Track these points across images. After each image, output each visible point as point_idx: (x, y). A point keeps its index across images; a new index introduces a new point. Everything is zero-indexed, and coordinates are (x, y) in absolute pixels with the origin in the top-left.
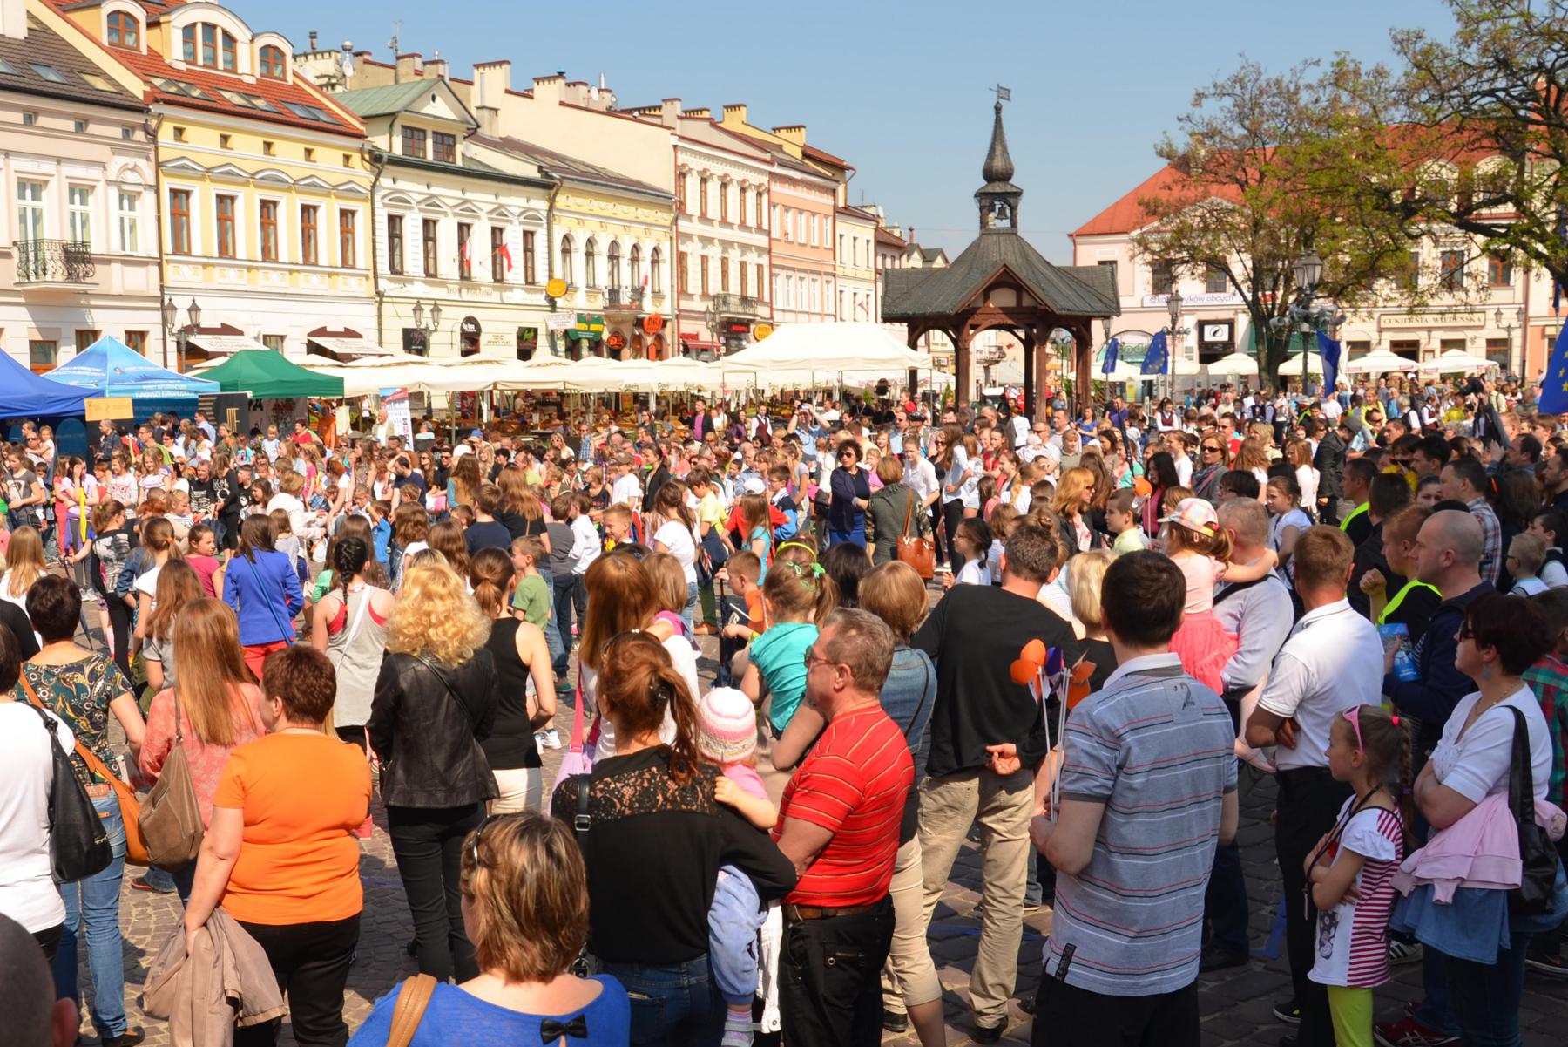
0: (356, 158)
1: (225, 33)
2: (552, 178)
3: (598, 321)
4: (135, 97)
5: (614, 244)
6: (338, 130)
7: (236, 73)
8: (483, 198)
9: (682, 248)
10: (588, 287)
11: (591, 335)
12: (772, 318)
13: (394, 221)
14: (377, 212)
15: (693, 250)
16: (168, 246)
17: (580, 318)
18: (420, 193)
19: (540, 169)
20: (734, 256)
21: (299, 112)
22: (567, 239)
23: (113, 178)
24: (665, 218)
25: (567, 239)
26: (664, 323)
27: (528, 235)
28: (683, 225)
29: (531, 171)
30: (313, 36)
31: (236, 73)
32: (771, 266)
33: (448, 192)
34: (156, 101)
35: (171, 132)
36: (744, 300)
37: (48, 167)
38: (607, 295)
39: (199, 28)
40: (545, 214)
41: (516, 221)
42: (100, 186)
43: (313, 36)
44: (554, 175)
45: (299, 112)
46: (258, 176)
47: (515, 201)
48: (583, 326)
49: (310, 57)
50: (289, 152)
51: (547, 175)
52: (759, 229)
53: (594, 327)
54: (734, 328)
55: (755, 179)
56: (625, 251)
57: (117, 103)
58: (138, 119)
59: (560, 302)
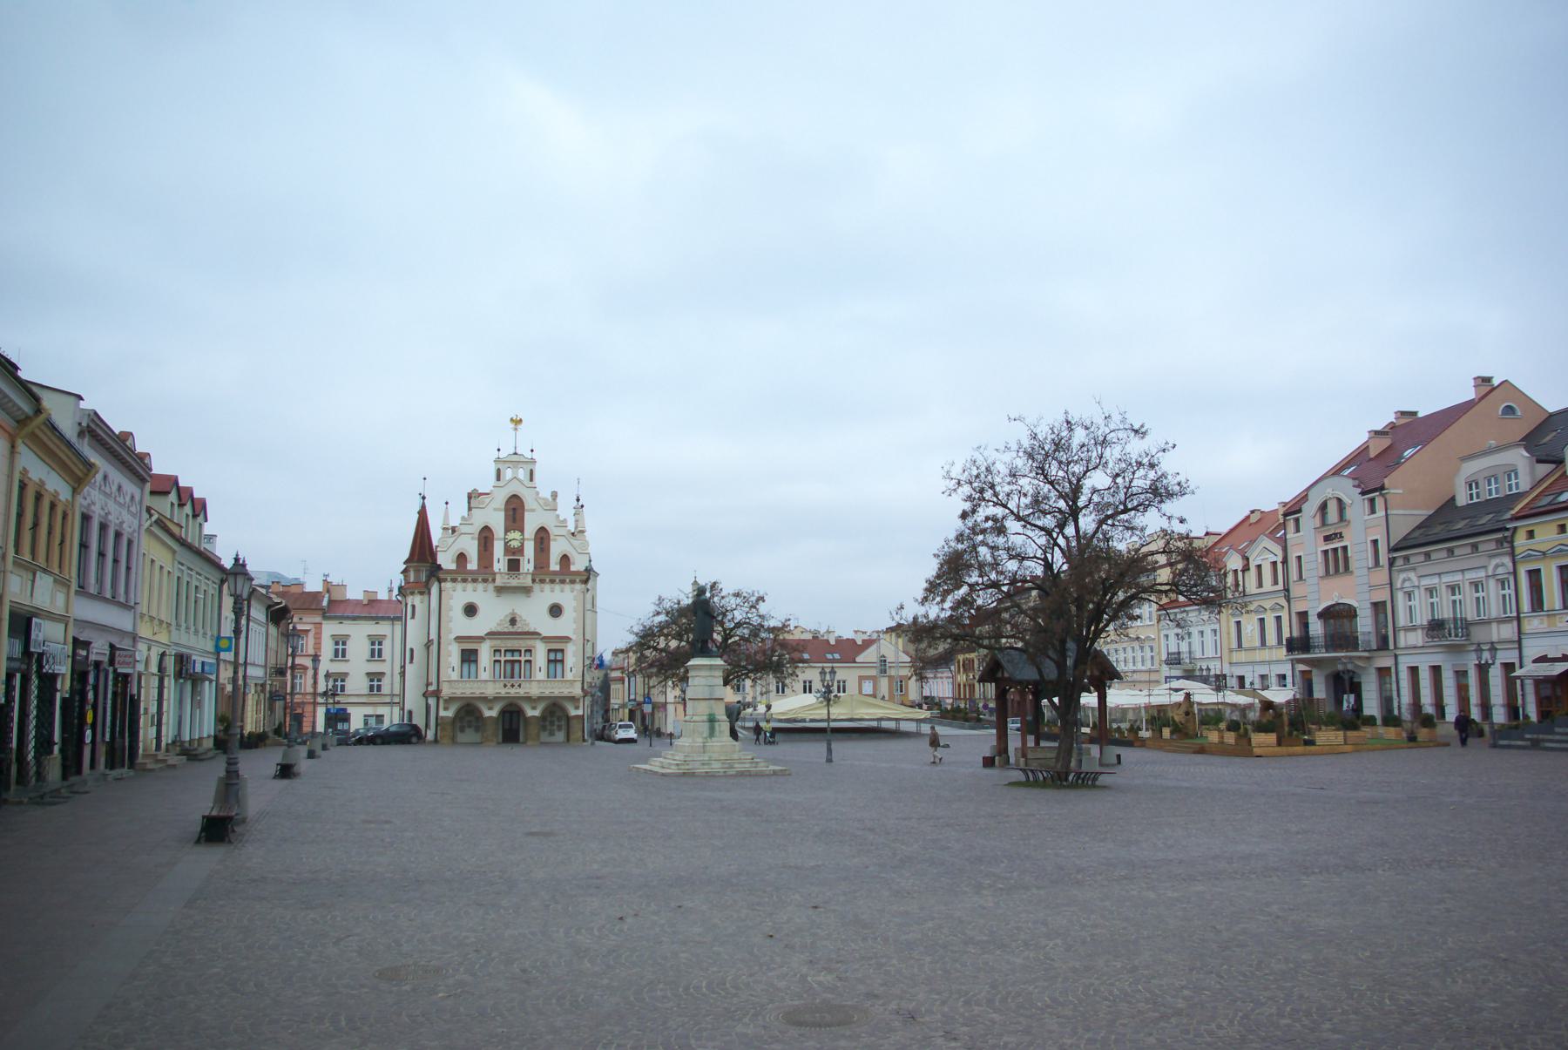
23: (1490, 574)
37: (1435, 580)
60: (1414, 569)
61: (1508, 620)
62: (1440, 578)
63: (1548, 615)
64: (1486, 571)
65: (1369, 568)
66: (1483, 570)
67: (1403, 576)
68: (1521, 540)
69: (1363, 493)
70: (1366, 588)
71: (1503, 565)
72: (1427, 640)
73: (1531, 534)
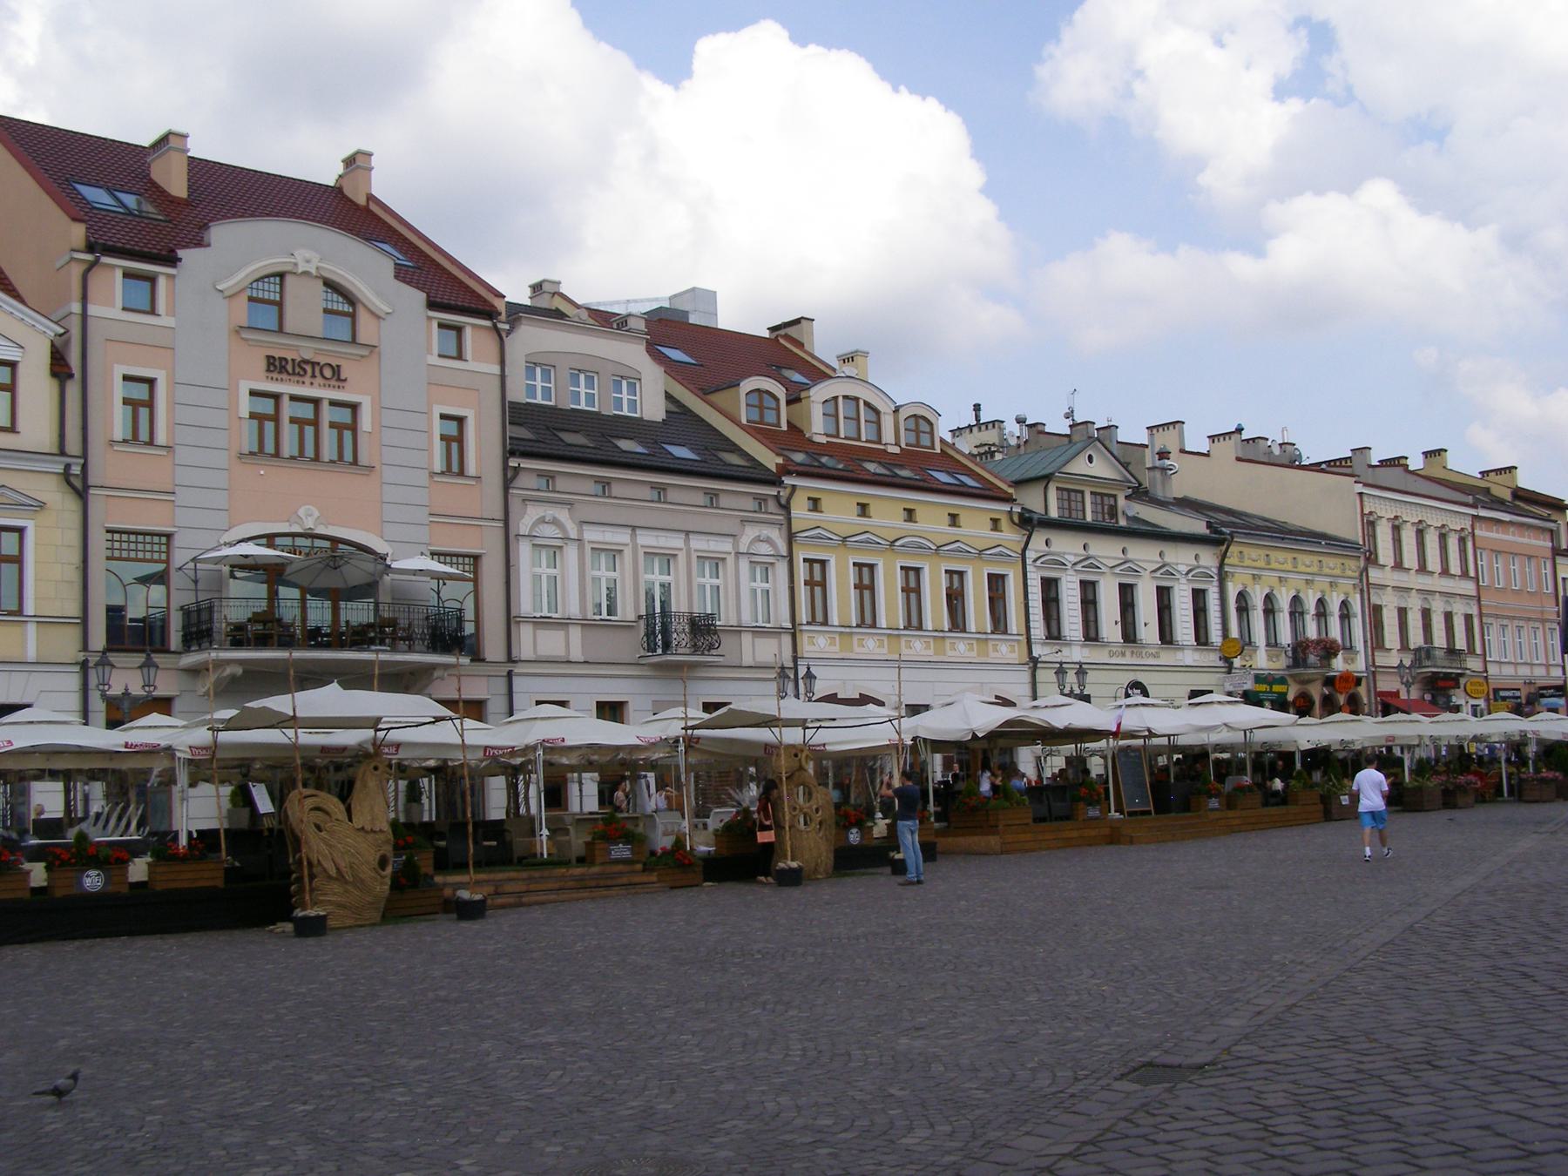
0: (1004, 523)
1: (867, 404)
2: (1222, 533)
3: (1282, 681)
4: (769, 470)
5: (1296, 600)
6: (988, 493)
7: (879, 442)
8: (1145, 554)
9: (1375, 600)
10: (1268, 645)
11: (1274, 697)
12: (1486, 671)
13: (1050, 586)
14: (1029, 575)
15: (1389, 604)
16: (803, 615)
17: (1258, 679)
18: (1076, 555)
19: (1209, 525)
20: (1438, 607)
21: (944, 478)
22: (1242, 596)
23: (743, 549)
24: (1353, 566)
25: (1242, 596)
26: (1358, 681)
27: (1199, 596)
28: (1375, 575)
29: (1198, 526)
30: (977, 408)
31: (879, 442)
32: (1481, 615)
33: (1106, 550)
34: (789, 473)
35: (806, 504)
36: (1451, 651)
38: (1290, 654)
39: (840, 399)
40: (1215, 570)
41: (1183, 580)
42: (730, 560)
43: (977, 408)
44: (1224, 529)
45: (944, 478)
46: (897, 544)
47: (1182, 557)
48: (1263, 687)
49: (975, 429)
50: (932, 515)
51: (1216, 531)
52: (1465, 574)
53: (1276, 688)
54: (1441, 684)
55: (1456, 524)
57: (754, 475)
58: (773, 491)
59: (1237, 662)
60: (570, 504)
61: (776, 632)
62: (633, 536)
63: (978, 639)
64: (735, 545)
65: (433, 474)
66: (730, 540)
67: (533, 513)
68: (800, 510)
69: (432, 305)
70: (183, 496)
71: (768, 541)
72: (643, 653)
73: (815, 504)
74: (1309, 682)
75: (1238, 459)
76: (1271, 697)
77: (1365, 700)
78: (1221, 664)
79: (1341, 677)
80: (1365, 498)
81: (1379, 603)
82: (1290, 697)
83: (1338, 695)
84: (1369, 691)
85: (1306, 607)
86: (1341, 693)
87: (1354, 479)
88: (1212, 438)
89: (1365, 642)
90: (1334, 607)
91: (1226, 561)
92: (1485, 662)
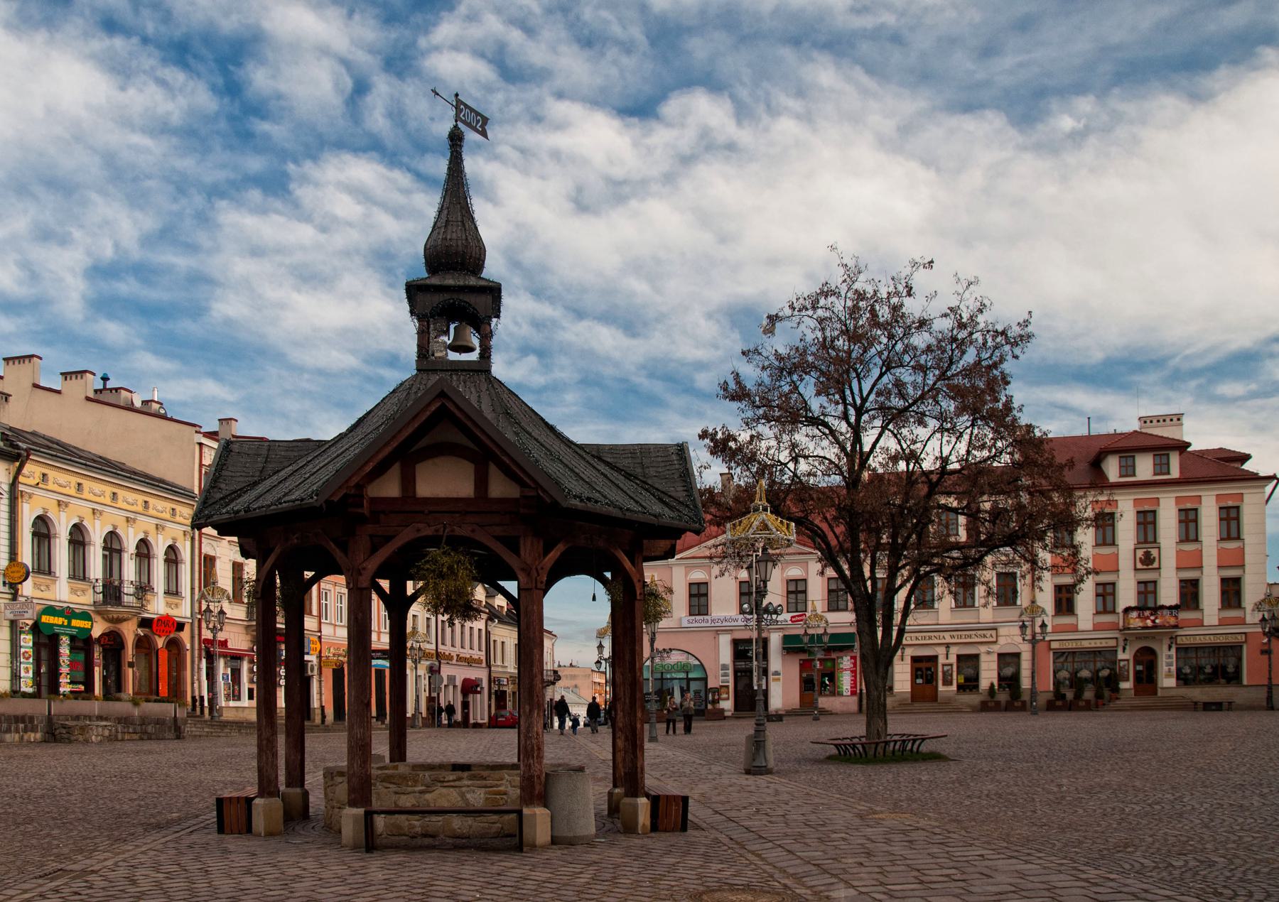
9: (207, 549)
11: (74, 632)
12: (320, 631)
17: (50, 610)
26: (180, 627)
38: (100, 589)
44: (20, 444)
53: (75, 623)
56: (130, 546)
74: (119, 621)
75: (88, 399)
76: (68, 631)
77: (188, 646)
78: (6, 589)
79: (159, 620)
80: (205, 450)
81: (212, 553)
82: (96, 633)
83: (157, 637)
84: (192, 637)
85: (125, 544)
86: (160, 636)
87: (195, 429)
88: (66, 375)
89: (192, 589)
90: (159, 550)
91: (21, 479)
92: (320, 623)
